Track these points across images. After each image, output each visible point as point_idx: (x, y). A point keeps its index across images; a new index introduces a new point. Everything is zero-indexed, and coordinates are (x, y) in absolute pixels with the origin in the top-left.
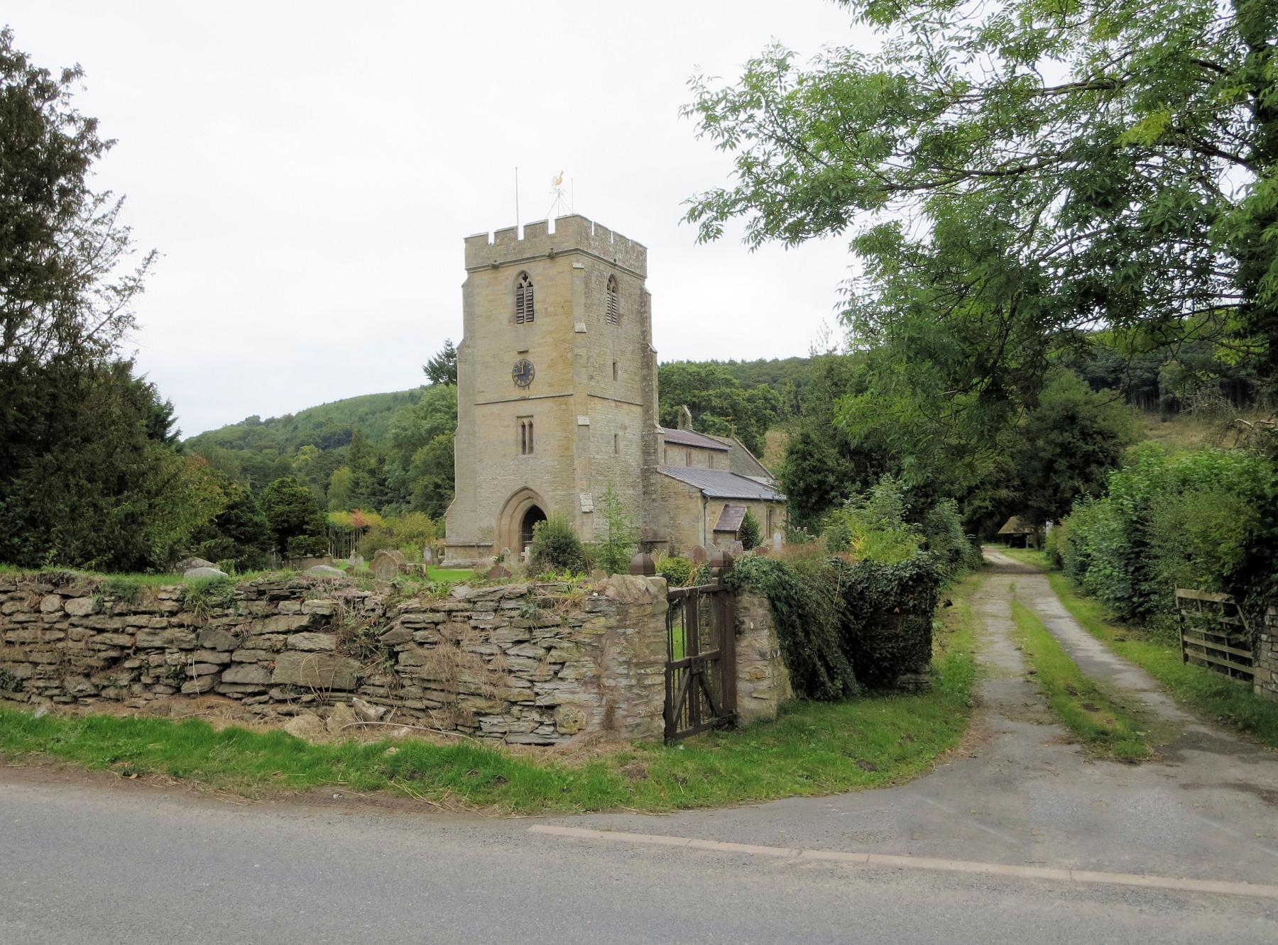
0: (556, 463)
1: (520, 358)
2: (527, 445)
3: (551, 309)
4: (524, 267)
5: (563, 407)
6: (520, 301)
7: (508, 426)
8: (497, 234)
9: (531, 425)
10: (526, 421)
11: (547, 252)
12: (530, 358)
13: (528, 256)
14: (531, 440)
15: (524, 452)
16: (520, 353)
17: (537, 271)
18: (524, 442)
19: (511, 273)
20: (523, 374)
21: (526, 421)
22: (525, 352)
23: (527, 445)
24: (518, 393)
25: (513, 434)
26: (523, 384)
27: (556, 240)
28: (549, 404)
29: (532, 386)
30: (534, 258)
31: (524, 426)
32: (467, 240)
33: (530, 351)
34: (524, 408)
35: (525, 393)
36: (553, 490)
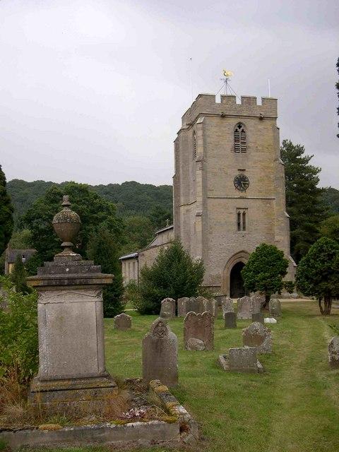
2: (241, 225)
6: (236, 140)
7: (231, 213)
8: (223, 97)
9: (244, 214)
10: (242, 211)
12: (246, 174)
14: (244, 223)
15: (239, 229)
16: (239, 170)
17: (250, 125)
18: (239, 224)
19: (234, 122)
20: (241, 182)
21: (242, 211)
23: (241, 225)
24: (238, 194)
25: (234, 219)
28: (259, 203)
31: (239, 214)
32: (271, 102)
34: (241, 203)
35: (242, 194)
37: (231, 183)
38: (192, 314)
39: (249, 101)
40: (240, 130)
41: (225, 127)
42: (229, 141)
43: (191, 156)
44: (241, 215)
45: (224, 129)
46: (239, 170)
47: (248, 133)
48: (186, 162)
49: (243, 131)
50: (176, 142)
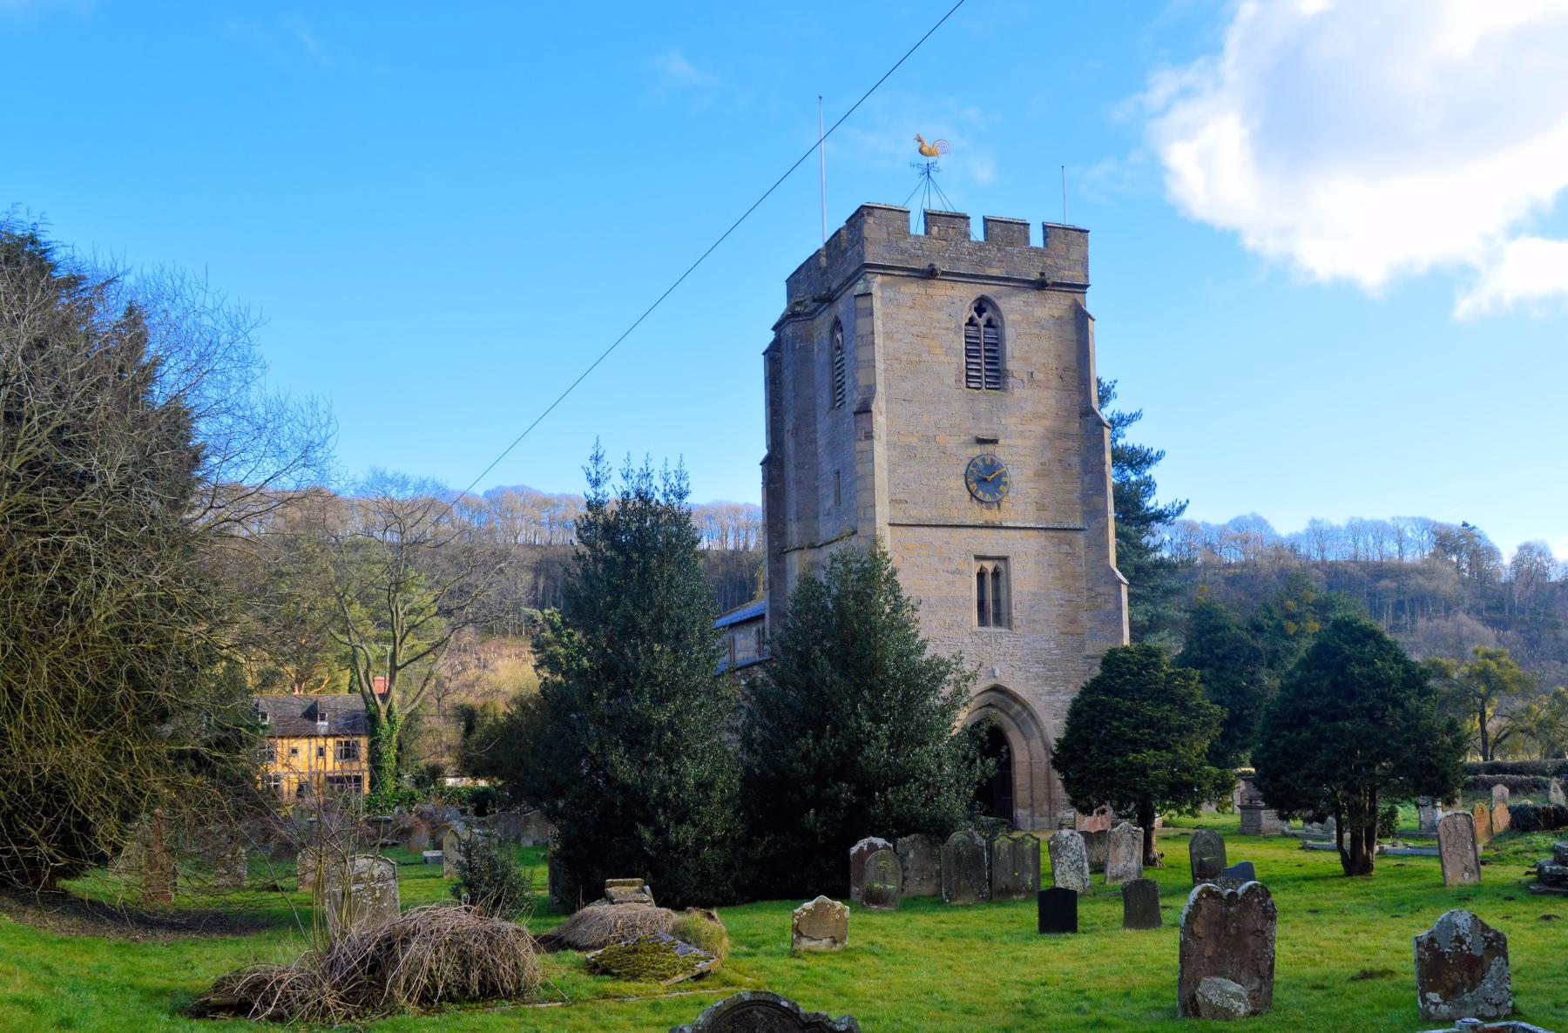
0: (1052, 645)
1: (977, 450)
3: (1038, 376)
4: (988, 290)
5: (1065, 548)
7: (959, 572)
11: (1035, 276)
12: (1001, 453)
13: (995, 272)
14: (997, 601)
15: (983, 620)
16: (981, 441)
19: (966, 294)
21: (989, 566)
22: (994, 442)
26: (988, 498)
27: (1049, 261)
29: (1003, 505)
30: (1008, 279)
31: (981, 575)
33: (1000, 442)
34: (992, 543)
36: (1049, 693)
37: (956, 485)
38: (1209, 892)
39: (1005, 232)
40: (982, 321)
41: (939, 310)
42: (950, 355)
43: (824, 398)
44: (989, 579)
45: (935, 315)
46: (981, 441)
47: (1009, 332)
48: (806, 419)
49: (989, 324)
50: (774, 355)
